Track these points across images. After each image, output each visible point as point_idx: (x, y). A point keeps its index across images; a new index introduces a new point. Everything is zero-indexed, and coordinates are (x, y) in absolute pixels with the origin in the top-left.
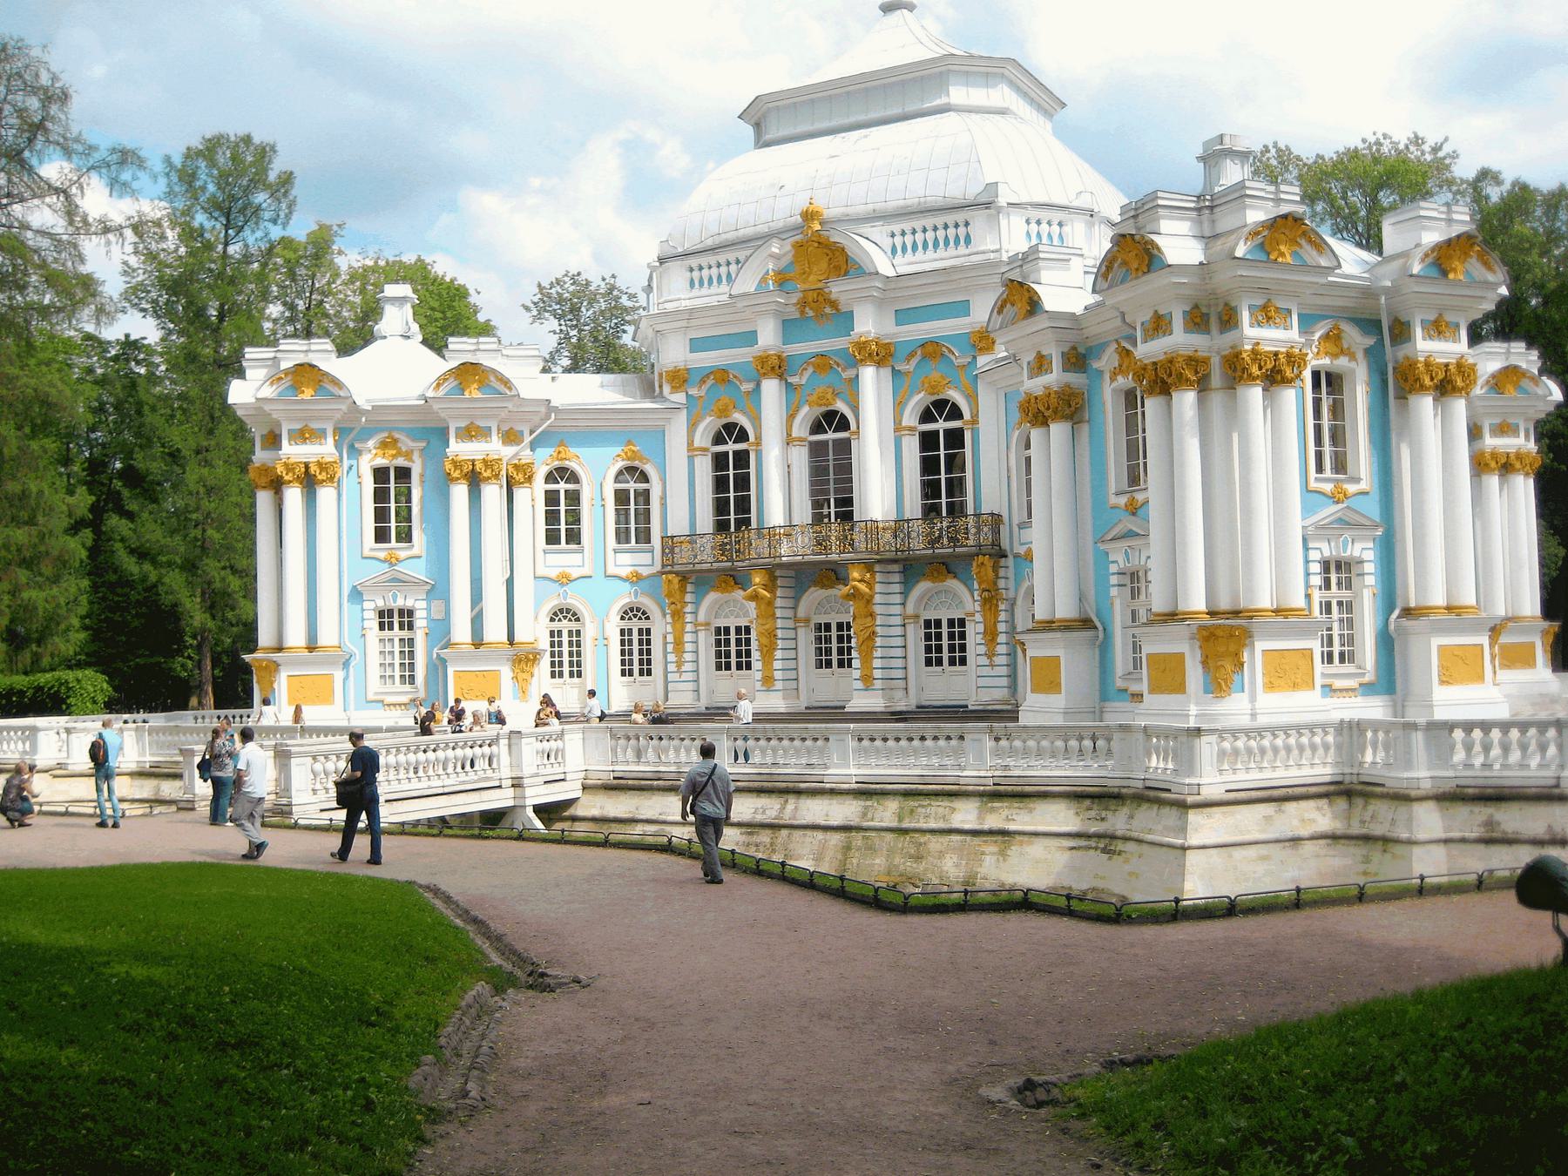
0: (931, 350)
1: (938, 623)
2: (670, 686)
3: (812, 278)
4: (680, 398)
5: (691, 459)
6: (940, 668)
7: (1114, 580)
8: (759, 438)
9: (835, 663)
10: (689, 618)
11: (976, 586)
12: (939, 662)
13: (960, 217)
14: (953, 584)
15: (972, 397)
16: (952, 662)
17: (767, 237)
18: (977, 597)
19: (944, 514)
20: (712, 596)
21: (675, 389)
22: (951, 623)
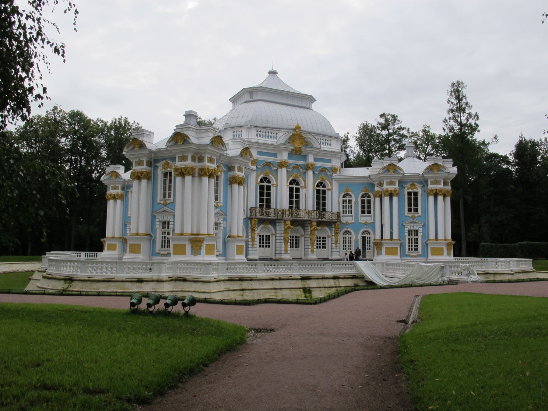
0: (323, 170)
1: (320, 238)
2: (249, 252)
3: (296, 144)
4: (254, 167)
5: (256, 185)
6: (320, 249)
7: (407, 231)
8: (277, 183)
9: (294, 247)
10: (256, 232)
11: (333, 229)
12: (320, 248)
13: (329, 139)
14: (326, 228)
15: (331, 183)
16: (323, 248)
17: (280, 129)
18: (333, 232)
19: (321, 210)
20: (262, 226)
21: (252, 164)
22: (323, 238)
